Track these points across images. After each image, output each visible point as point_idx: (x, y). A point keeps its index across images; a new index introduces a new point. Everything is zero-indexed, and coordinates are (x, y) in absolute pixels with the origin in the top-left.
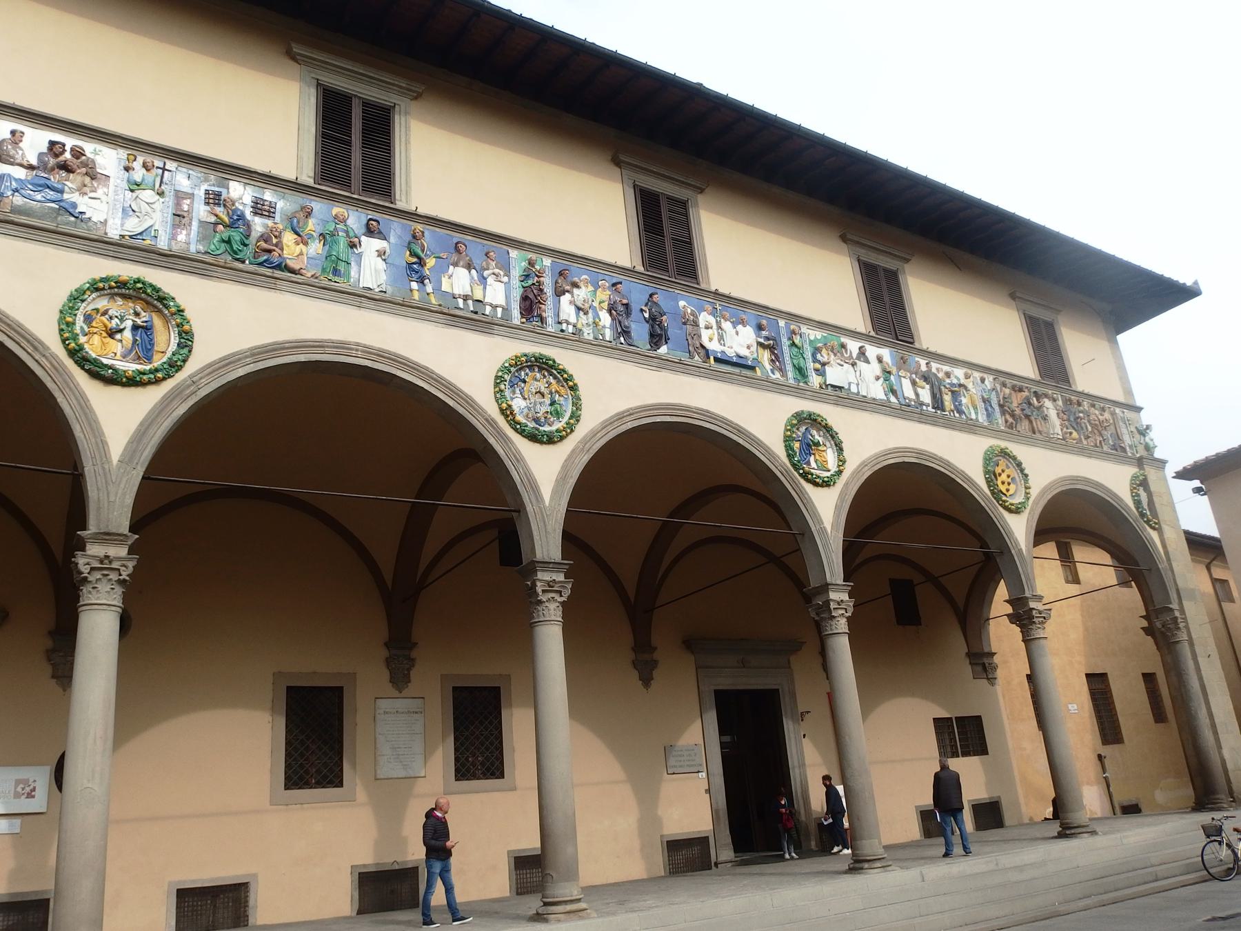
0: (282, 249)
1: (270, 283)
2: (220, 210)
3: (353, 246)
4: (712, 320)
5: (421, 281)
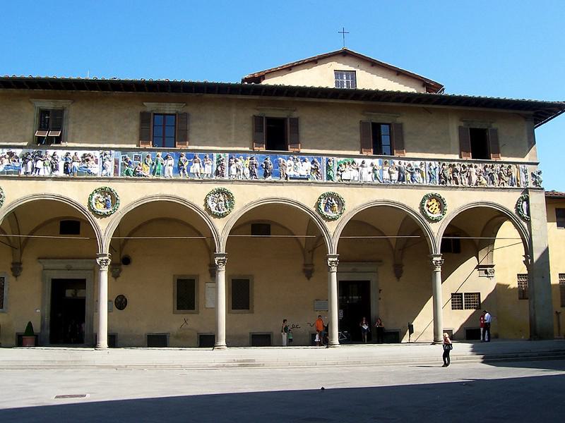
4: (292, 163)
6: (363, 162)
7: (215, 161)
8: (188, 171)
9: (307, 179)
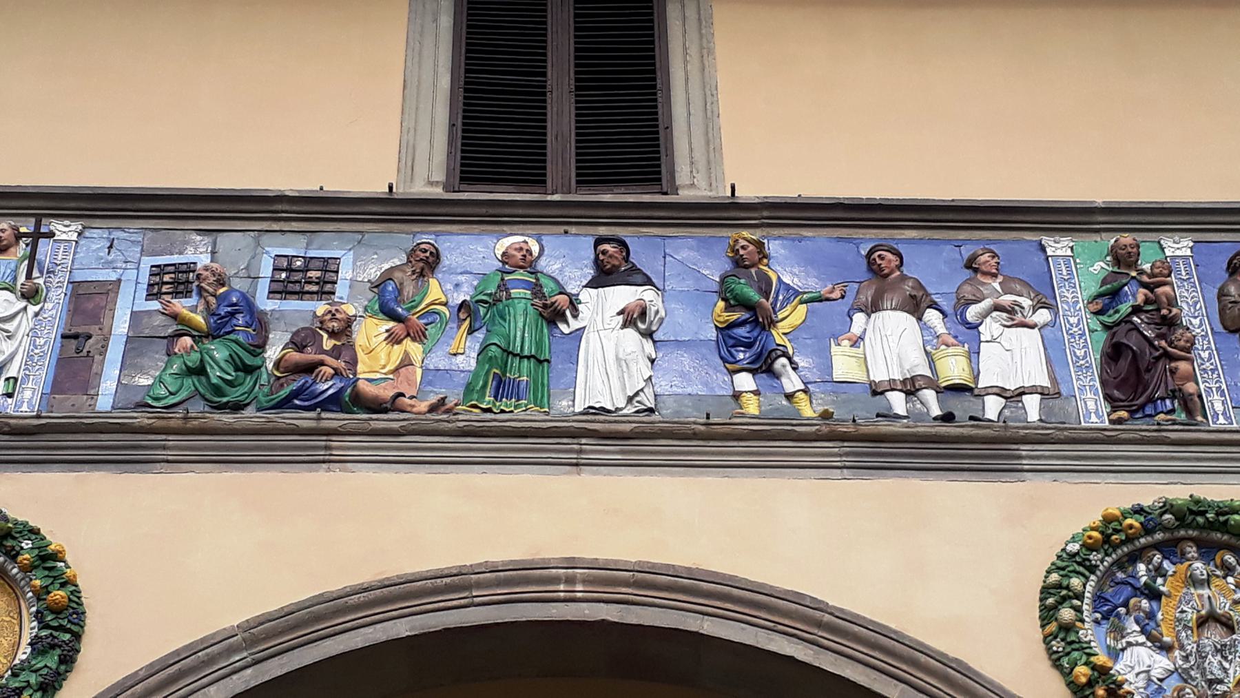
0: (353, 362)
1: (315, 449)
2: (182, 305)
3: (553, 316)
5: (764, 365)
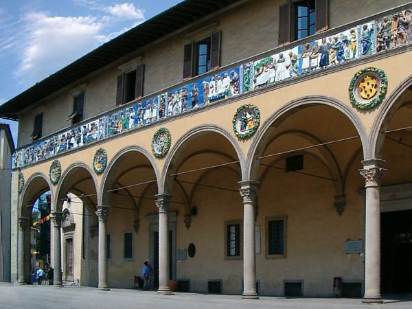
6: (281, 57)
7: (159, 102)
8: (143, 119)
9: (224, 97)
